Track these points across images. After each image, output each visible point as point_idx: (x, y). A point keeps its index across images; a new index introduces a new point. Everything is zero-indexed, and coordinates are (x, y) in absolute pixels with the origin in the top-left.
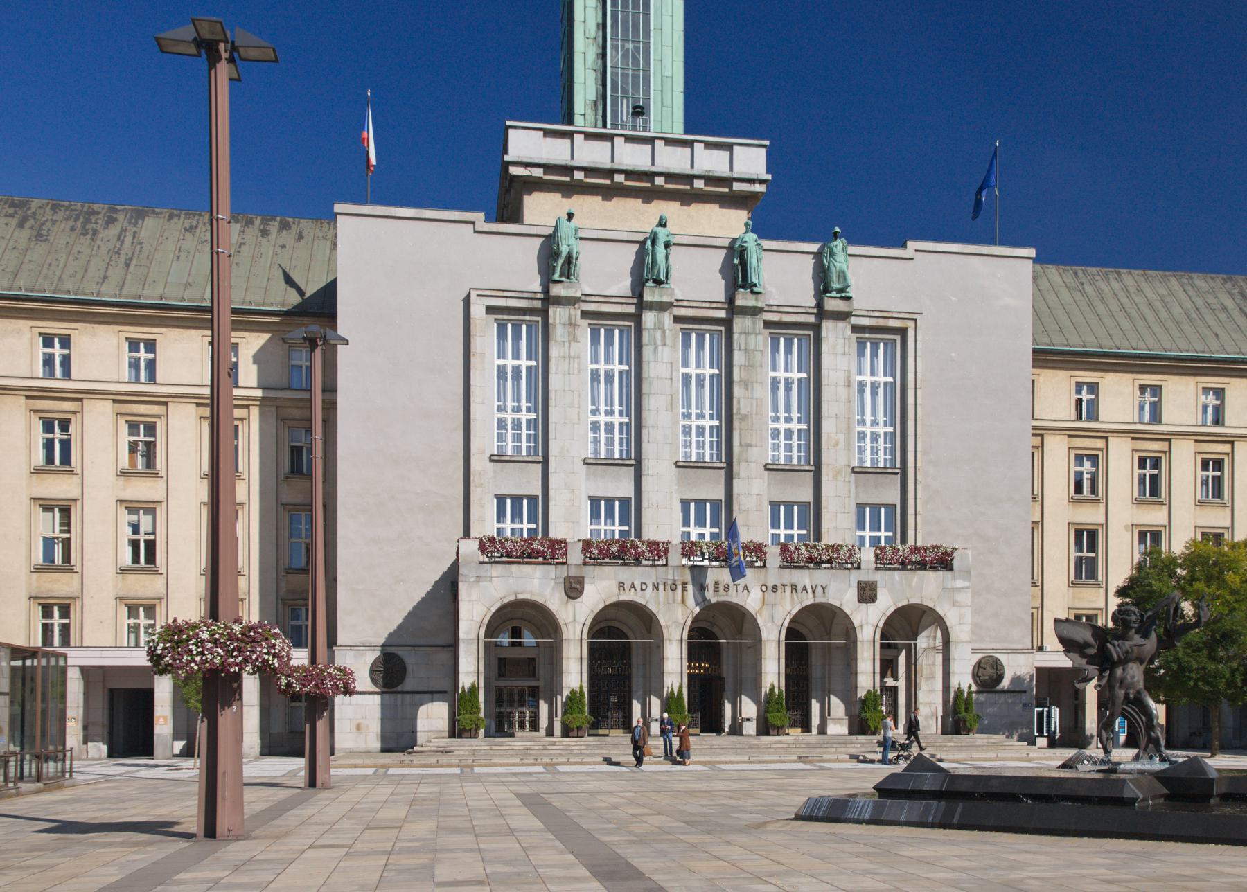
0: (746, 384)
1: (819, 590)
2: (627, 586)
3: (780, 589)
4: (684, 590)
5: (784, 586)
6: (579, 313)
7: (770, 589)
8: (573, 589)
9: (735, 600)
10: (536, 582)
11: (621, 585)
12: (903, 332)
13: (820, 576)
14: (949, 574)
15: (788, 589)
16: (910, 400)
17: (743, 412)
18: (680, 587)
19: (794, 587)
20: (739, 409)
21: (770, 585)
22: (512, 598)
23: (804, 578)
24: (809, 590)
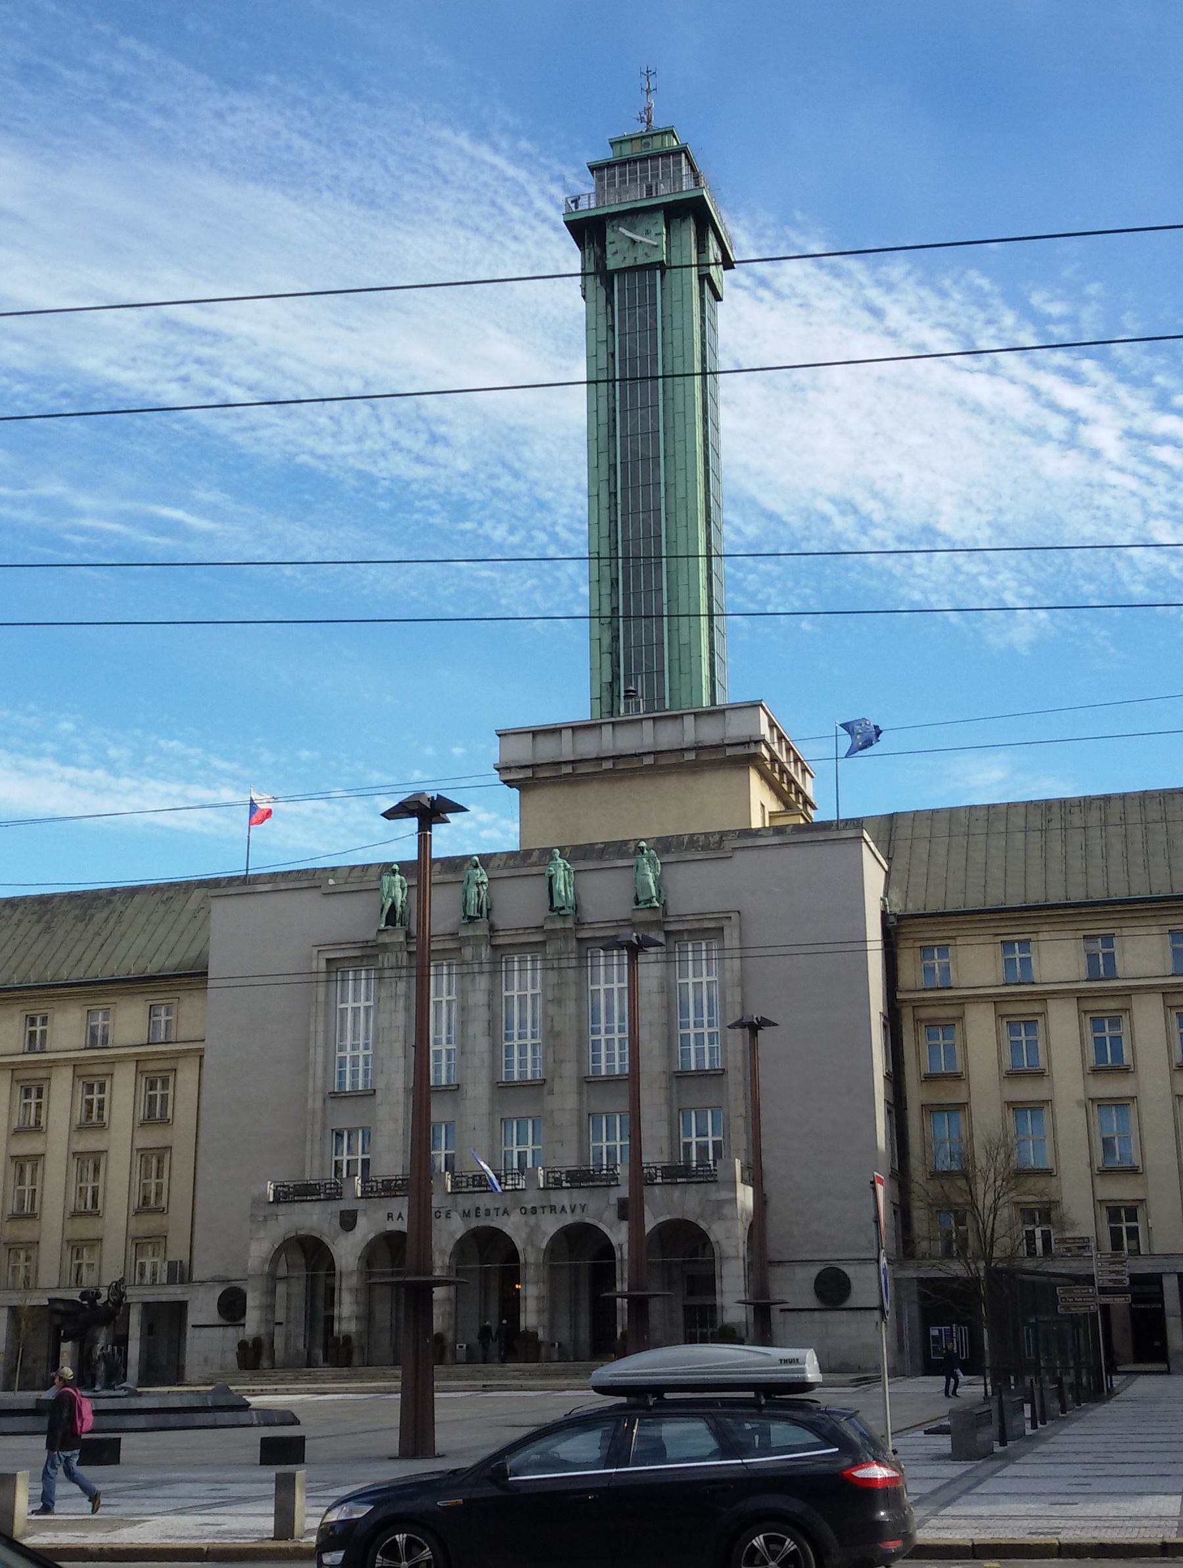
0: (559, 1002)
1: (578, 1210)
2: (395, 1216)
3: (539, 1211)
4: (448, 1216)
5: (543, 1207)
6: (405, 954)
7: (529, 1212)
8: (348, 1221)
9: (493, 1224)
10: (315, 1217)
11: (390, 1216)
12: (722, 929)
13: (579, 1197)
14: (712, 1187)
15: (547, 1210)
16: (729, 999)
17: (557, 1029)
18: (443, 1215)
19: (553, 1209)
20: (552, 1027)
21: (529, 1207)
22: (293, 1234)
23: (562, 1198)
24: (568, 1210)
